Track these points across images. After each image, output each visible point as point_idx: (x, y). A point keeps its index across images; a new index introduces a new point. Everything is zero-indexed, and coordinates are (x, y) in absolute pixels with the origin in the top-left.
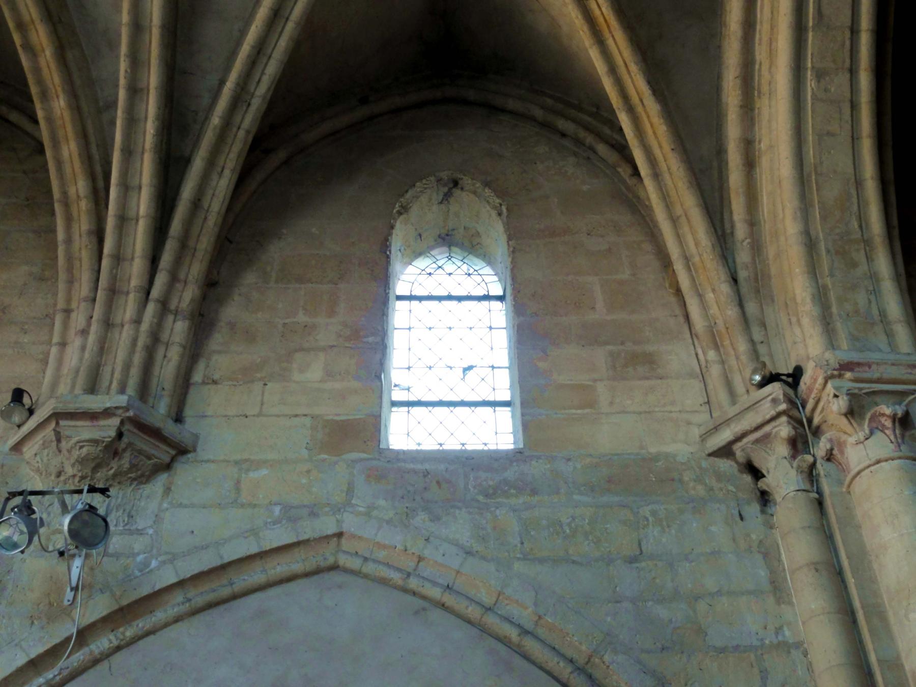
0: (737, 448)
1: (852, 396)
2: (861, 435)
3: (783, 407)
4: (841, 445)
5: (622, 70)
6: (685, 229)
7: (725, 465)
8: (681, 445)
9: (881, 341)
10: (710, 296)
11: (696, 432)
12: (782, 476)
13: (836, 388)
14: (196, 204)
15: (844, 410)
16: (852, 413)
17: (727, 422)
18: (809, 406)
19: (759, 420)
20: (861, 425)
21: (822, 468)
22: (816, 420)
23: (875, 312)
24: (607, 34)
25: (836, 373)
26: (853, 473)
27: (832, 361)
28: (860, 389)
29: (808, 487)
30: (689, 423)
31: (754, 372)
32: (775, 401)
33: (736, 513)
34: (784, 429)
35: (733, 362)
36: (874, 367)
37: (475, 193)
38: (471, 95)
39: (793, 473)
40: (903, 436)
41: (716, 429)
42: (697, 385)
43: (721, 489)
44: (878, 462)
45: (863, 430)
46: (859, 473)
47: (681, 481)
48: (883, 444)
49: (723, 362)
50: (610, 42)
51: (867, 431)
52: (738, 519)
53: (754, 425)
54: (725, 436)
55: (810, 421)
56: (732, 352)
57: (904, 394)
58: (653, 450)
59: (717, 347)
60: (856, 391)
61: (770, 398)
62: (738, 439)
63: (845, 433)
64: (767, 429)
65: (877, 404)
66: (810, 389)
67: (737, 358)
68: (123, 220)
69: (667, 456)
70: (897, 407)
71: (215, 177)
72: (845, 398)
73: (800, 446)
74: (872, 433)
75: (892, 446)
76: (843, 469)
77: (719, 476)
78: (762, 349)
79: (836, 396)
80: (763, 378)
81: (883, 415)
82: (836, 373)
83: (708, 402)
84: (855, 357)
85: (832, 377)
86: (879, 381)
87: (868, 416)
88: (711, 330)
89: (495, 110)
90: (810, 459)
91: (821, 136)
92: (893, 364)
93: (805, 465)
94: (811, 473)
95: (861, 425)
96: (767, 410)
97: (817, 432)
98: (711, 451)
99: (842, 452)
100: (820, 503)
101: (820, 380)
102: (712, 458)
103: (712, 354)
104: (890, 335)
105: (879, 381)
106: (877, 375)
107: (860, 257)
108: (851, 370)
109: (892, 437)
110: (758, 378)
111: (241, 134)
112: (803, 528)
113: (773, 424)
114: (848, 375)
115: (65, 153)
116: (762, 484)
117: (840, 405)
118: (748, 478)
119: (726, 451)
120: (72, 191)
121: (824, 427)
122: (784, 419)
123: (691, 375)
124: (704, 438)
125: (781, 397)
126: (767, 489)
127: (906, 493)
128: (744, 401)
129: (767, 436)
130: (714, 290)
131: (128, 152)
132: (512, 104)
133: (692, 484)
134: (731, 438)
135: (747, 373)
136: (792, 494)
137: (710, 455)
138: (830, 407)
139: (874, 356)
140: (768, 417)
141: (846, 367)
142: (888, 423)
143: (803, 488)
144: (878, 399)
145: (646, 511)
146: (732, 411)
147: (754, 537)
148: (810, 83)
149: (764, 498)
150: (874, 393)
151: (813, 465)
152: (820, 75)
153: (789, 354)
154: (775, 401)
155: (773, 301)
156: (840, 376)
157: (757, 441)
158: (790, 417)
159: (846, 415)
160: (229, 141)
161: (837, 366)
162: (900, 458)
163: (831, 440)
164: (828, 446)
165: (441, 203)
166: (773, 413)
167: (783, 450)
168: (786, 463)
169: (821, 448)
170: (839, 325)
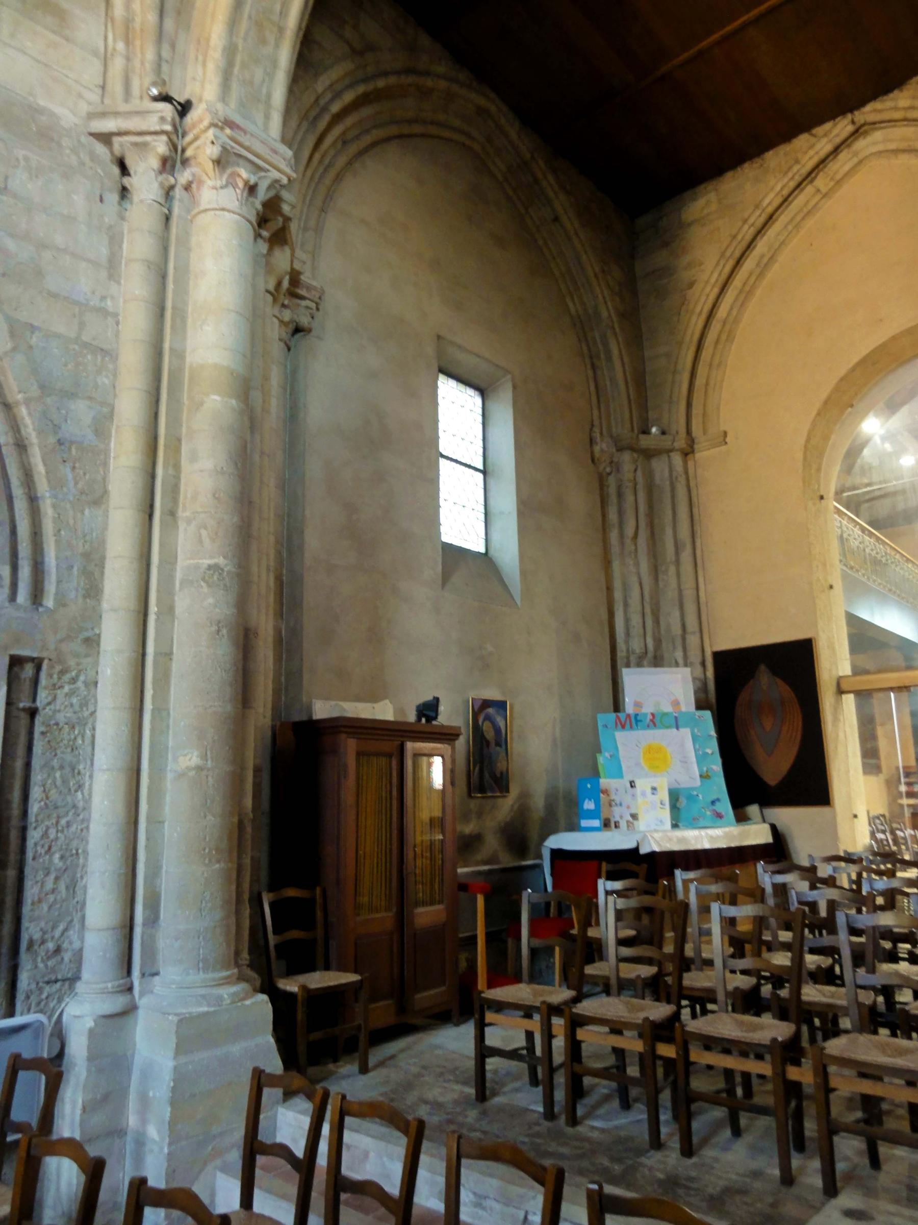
0: (116, 140)
1: (224, 149)
2: (219, 183)
3: (168, 128)
4: (200, 183)
7: (100, 149)
8: (68, 113)
9: (259, 118)
11: (84, 108)
12: (145, 182)
13: (215, 137)
15: (215, 157)
16: (218, 163)
17: (116, 114)
18: (188, 138)
19: (144, 127)
20: (221, 174)
21: (178, 193)
22: (189, 153)
23: (264, 91)
25: (220, 124)
26: (202, 208)
27: (220, 113)
28: (232, 148)
29: (162, 202)
30: (80, 96)
31: (154, 84)
32: (163, 119)
33: (98, 193)
34: (161, 147)
35: (137, 63)
36: (248, 136)
39: (156, 185)
40: (247, 200)
41: (103, 115)
42: (97, 65)
43: (91, 168)
44: (223, 209)
45: (221, 179)
46: (206, 210)
47: (59, 145)
48: (231, 198)
49: (128, 59)
51: (224, 182)
52: (98, 199)
53: (139, 130)
54: (109, 125)
55: (183, 151)
56: (139, 55)
57: (260, 168)
58: (42, 102)
59: (128, 42)
60: (229, 148)
61: (160, 114)
62: (120, 134)
63: (207, 175)
64: (148, 138)
65: (238, 165)
66: (194, 126)
67: (142, 63)
69: (52, 115)
70: (252, 176)
72: (220, 148)
73: (168, 165)
74: (226, 186)
75: (237, 203)
76: (194, 201)
77: (93, 156)
78: (165, 68)
79: (213, 143)
80: (160, 94)
81: (239, 176)
82: (220, 124)
83: (103, 87)
84: (238, 119)
85: (216, 126)
86: (248, 149)
87: (229, 171)
88: (128, 22)
90: (172, 180)
92: (262, 142)
93: (167, 184)
94: (168, 192)
95: (221, 174)
96: (152, 123)
97: (185, 162)
98: (93, 130)
99: (198, 189)
100: (167, 219)
101: (206, 123)
102: (91, 138)
103: (121, 46)
104: (267, 117)
105: (248, 149)
106: (247, 144)
107: (271, 39)
108: (231, 128)
109: (239, 197)
110: (155, 92)
112: (149, 232)
113: (155, 137)
114: (228, 131)
116: (126, 181)
117: (213, 151)
118: (116, 171)
119: (106, 138)
121: (192, 162)
122: (164, 138)
123: (95, 53)
124: (91, 116)
125: (169, 119)
126: (129, 187)
127: (234, 242)
128: (136, 103)
129: (145, 145)
133: (68, 151)
134: (114, 130)
135: (147, 81)
136: (149, 201)
137: (91, 134)
138: (204, 147)
139: (251, 127)
140: (152, 129)
141: (229, 123)
142: (241, 184)
143: (159, 200)
144: (241, 162)
145: (20, 153)
146: (123, 107)
147: (106, 220)
149: (124, 192)
150: (240, 156)
151: (172, 187)
153: (185, 85)
154: (163, 119)
155: (189, 27)
156: (222, 129)
157: (136, 144)
158: (170, 140)
159: (213, 161)
161: (222, 119)
162: (239, 215)
163: (194, 175)
164: (190, 179)
166: (157, 128)
167: (155, 163)
168: (153, 174)
169: (184, 177)
170: (235, 85)
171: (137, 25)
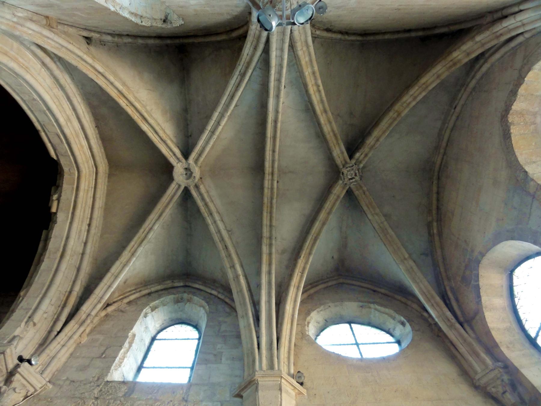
5: (108, 84)
6: (57, 45)
10: (30, 32)
14: (255, 49)
24: (118, 93)
37: (155, 19)
38: (169, 42)
50: (116, 91)
68: (282, 50)
71: (250, 54)
89: (159, 37)
91: (21, 85)
103: (15, 20)
111: (241, 65)
115: (307, 59)
120: (305, 49)
130: (30, 34)
131: (281, 66)
132: (151, 42)
148: (36, 97)
152: (34, 99)
160: (245, 64)
165: (169, 14)
171: (19, 27)
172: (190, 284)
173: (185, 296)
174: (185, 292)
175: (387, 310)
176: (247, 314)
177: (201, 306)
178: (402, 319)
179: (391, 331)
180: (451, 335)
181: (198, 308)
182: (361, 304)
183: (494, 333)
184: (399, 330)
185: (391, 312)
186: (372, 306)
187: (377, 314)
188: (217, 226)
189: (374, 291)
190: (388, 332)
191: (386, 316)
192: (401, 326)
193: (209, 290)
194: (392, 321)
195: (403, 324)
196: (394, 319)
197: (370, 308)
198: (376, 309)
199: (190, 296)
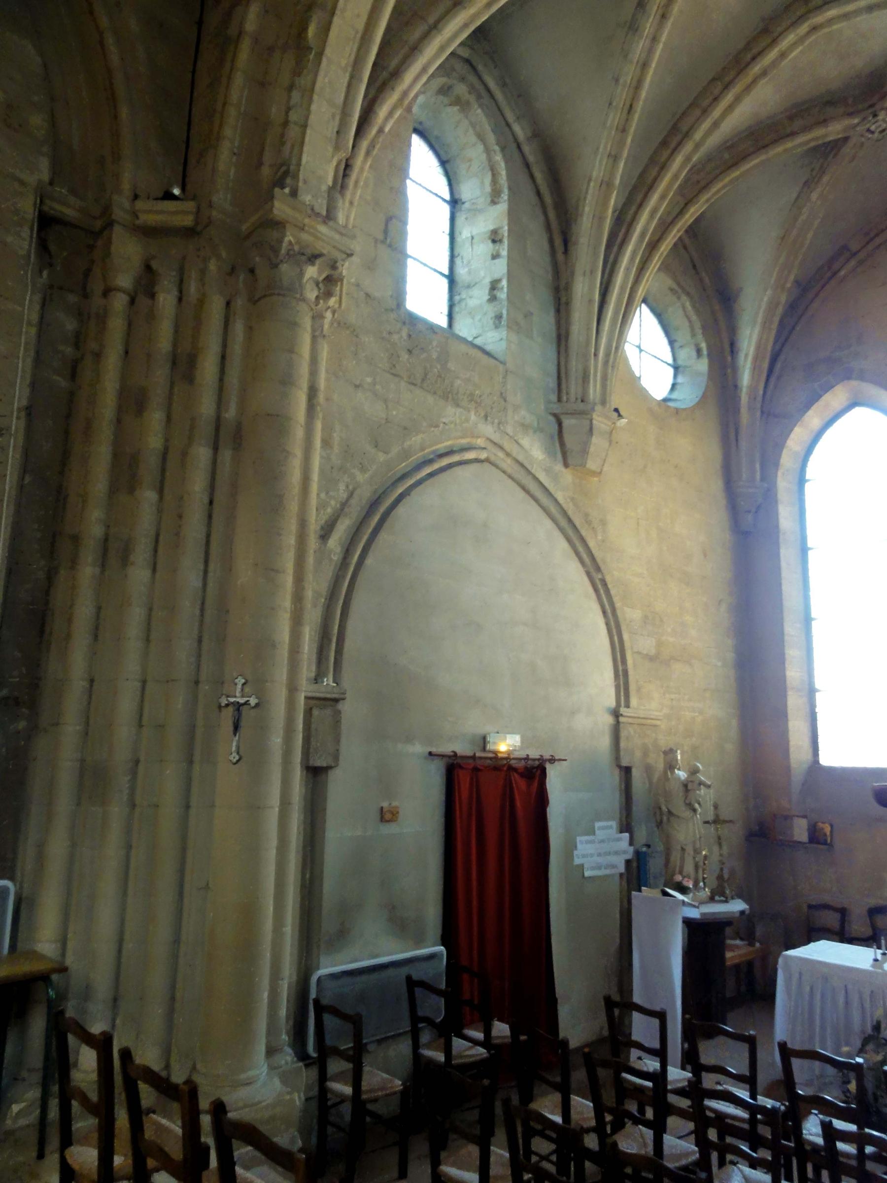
172: (480, 68)
173: (461, 89)
174: (463, 79)
175: (694, 318)
176: (592, 272)
177: (481, 137)
178: (704, 345)
179: (677, 345)
180: (745, 416)
181: (473, 139)
182: (675, 286)
183: (785, 452)
184: (687, 355)
185: (698, 325)
186: (684, 298)
187: (680, 312)
188: (650, 51)
189: (694, 266)
190: (671, 343)
191: (687, 324)
192: (694, 354)
193: (510, 116)
194: (688, 336)
195: (699, 351)
196: (693, 335)
197: (679, 298)
198: (684, 308)
199: (472, 99)
